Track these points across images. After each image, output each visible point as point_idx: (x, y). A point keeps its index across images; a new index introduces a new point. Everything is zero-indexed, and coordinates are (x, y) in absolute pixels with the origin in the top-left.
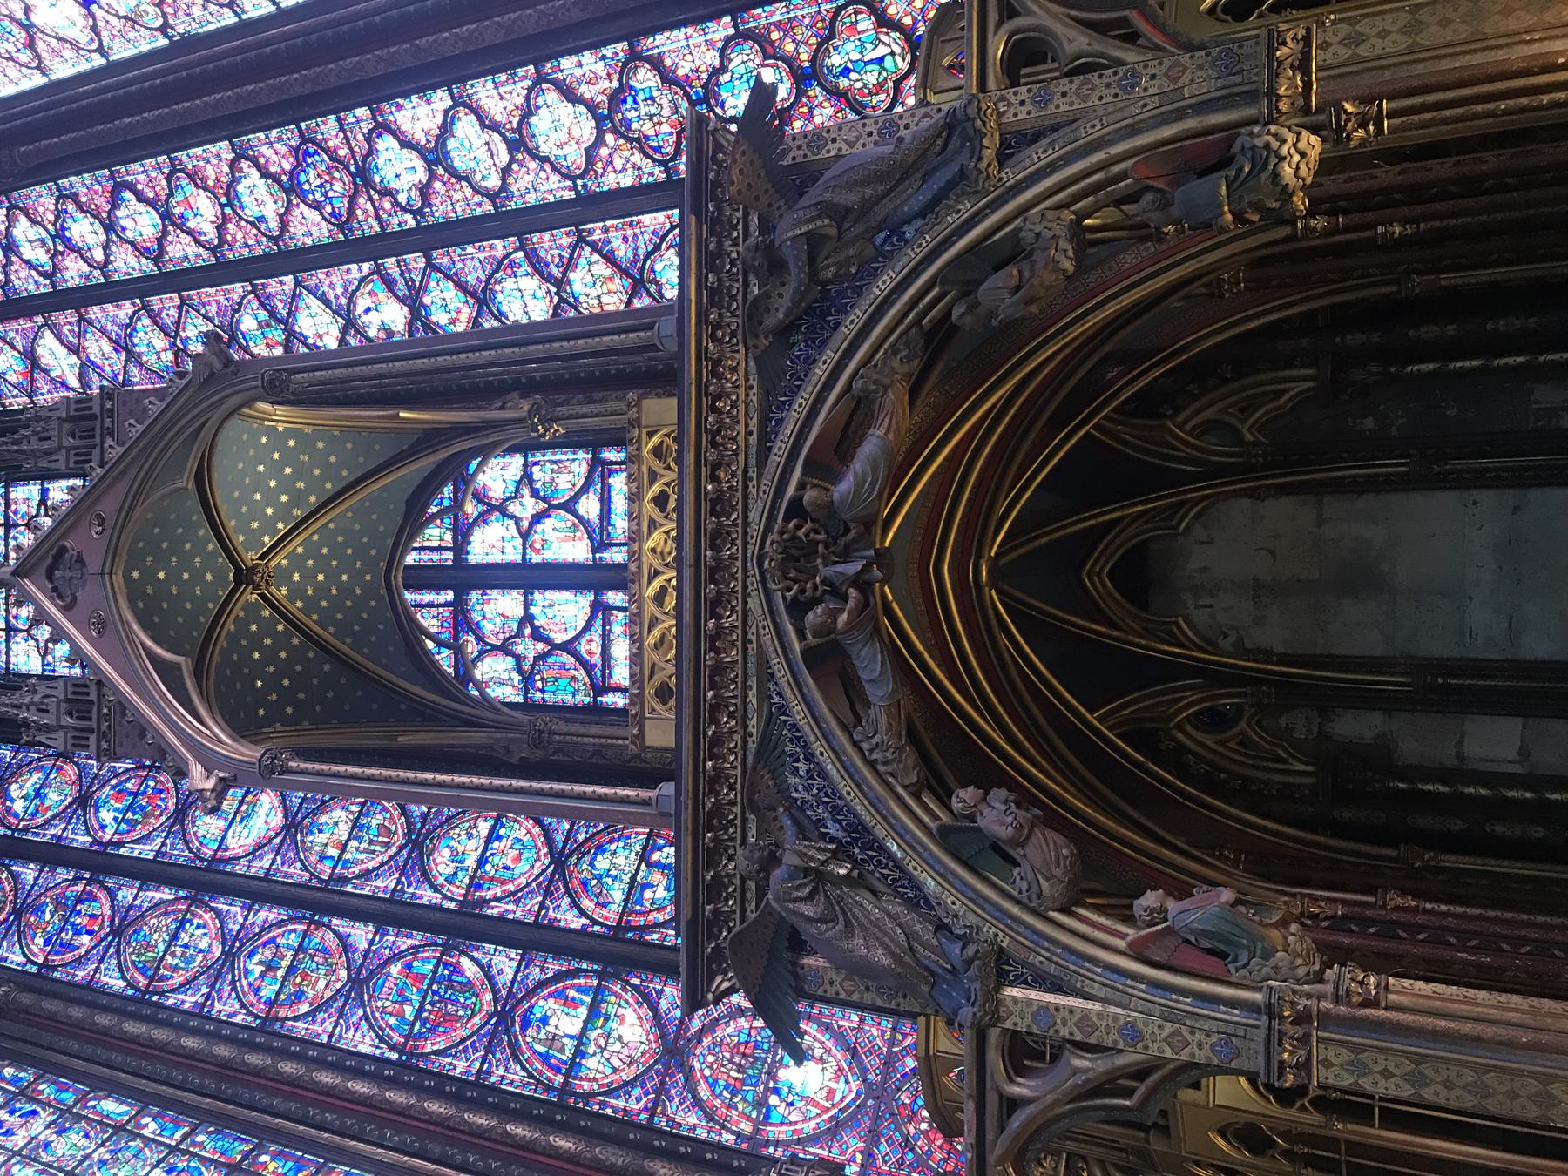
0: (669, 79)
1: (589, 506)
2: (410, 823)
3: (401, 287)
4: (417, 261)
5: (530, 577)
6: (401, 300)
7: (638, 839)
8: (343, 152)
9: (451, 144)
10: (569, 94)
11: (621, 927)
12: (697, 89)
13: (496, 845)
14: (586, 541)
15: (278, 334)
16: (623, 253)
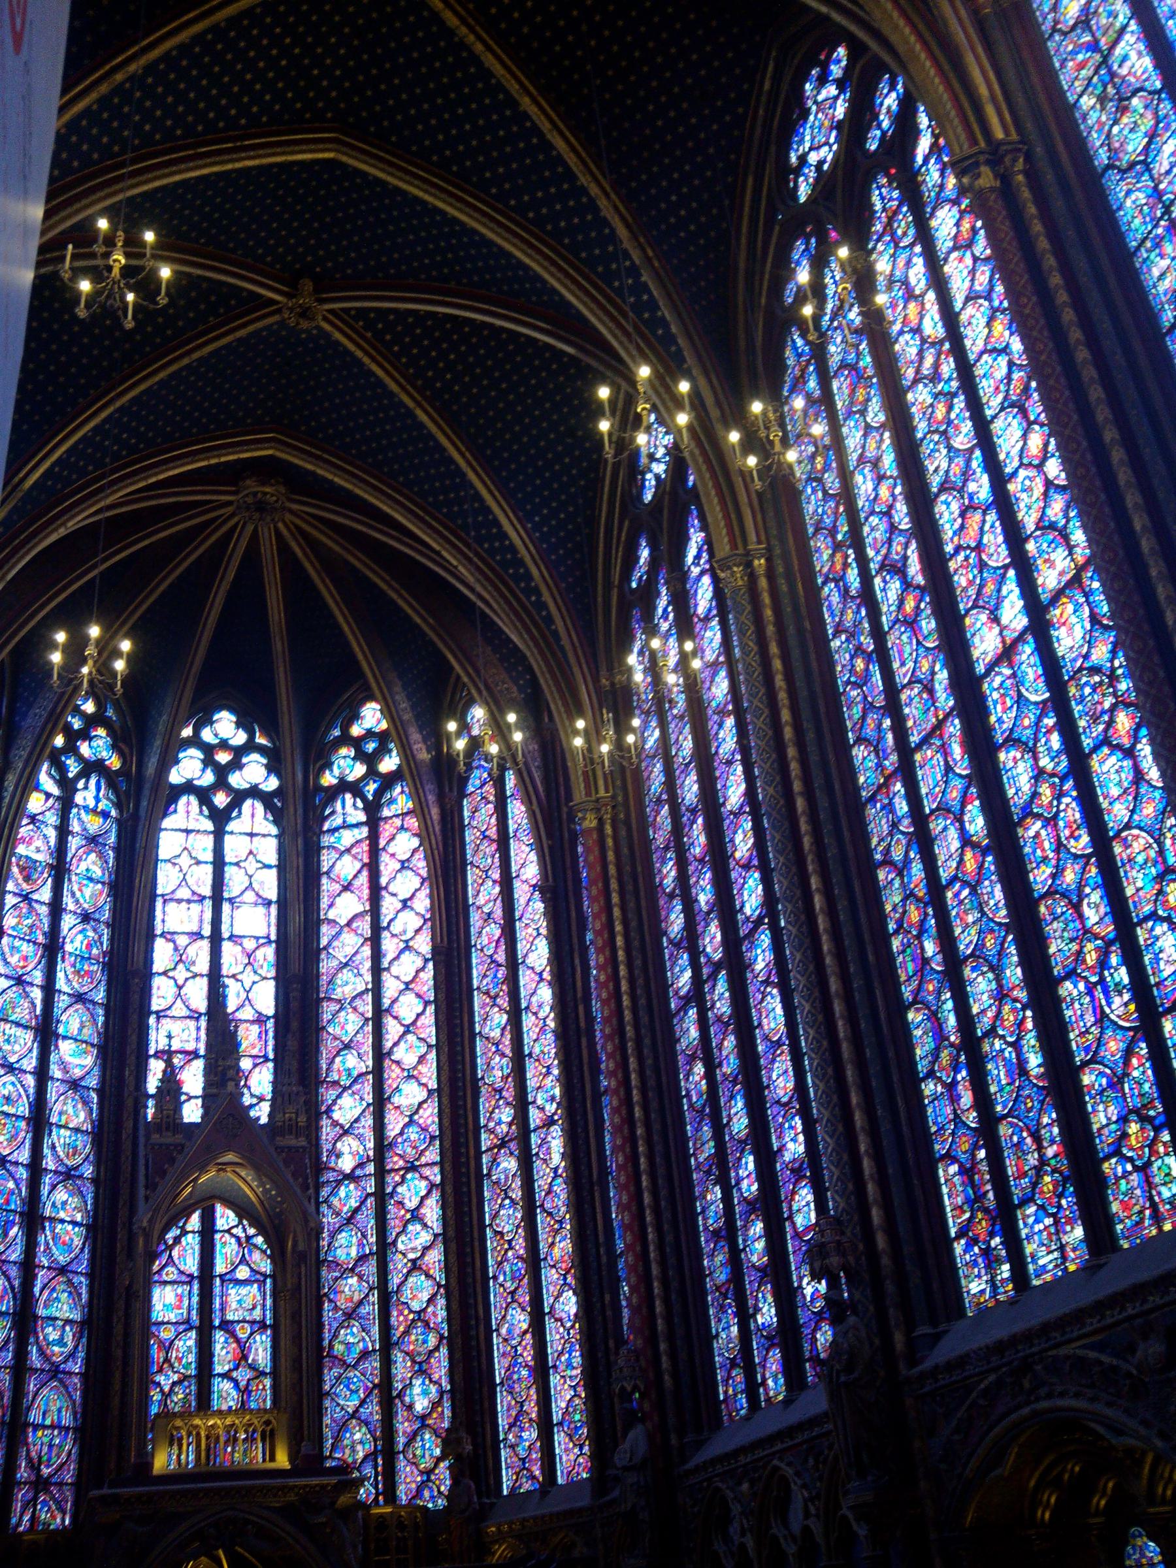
0: (431, 1353)
1: (243, 1273)
2: (76, 1168)
3: (358, 1172)
4: (370, 1186)
5: (208, 1233)
6: (353, 1170)
7: (76, 1316)
8: (423, 1160)
9: (418, 1227)
10: (431, 1301)
11: (36, 1317)
12: (425, 1366)
13: (70, 1227)
14: (224, 1271)
15: (345, 1082)
16: (364, 1310)
